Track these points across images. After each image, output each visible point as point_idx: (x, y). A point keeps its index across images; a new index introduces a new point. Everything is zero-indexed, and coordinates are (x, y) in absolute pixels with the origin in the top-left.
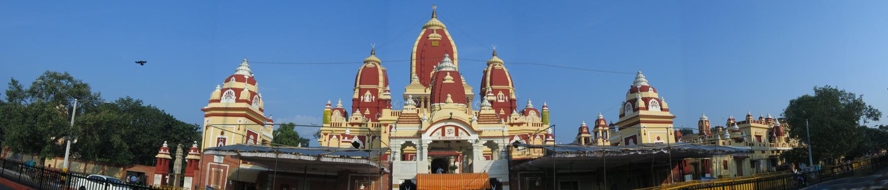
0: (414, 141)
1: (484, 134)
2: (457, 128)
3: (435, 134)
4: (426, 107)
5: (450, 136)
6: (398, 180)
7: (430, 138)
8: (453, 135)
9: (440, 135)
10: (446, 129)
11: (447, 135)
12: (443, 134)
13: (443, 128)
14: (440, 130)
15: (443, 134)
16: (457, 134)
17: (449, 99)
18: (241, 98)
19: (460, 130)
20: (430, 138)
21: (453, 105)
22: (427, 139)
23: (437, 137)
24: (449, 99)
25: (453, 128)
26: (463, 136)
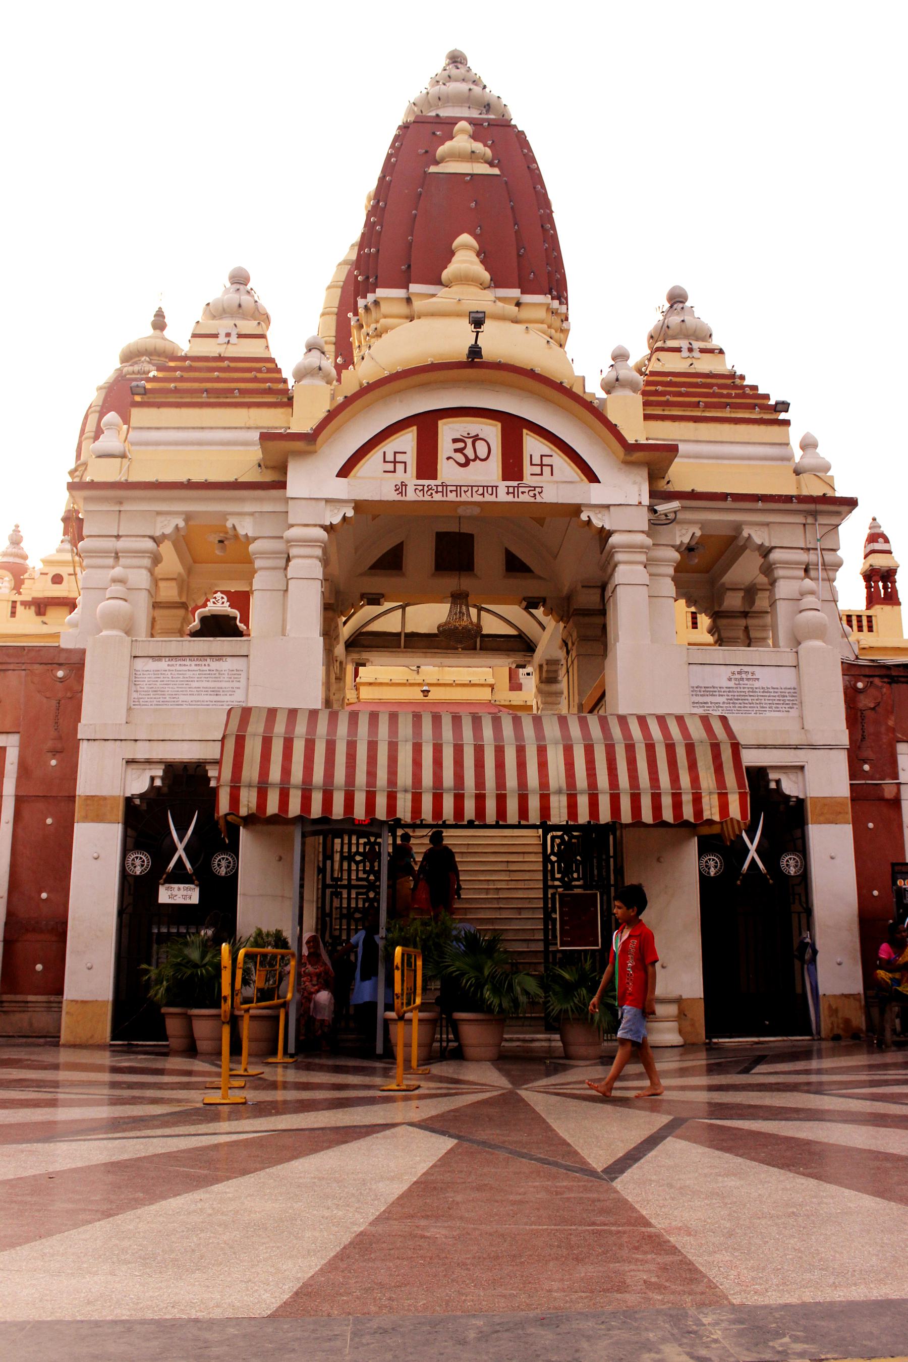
0: (246, 519)
1: (683, 475)
2: (513, 428)
3: (373, 463)
5: (472, 476)
6: (107, 773)
7: (342, 489)
8: (495, 465)
11: (448, 471)
12: (427, 466)
13: (426, 425)
14: (407, 442)
16: (512, 467)
19: (533, 446)
20: (342, 489)
25: (492, 432)
26: (556, 484)
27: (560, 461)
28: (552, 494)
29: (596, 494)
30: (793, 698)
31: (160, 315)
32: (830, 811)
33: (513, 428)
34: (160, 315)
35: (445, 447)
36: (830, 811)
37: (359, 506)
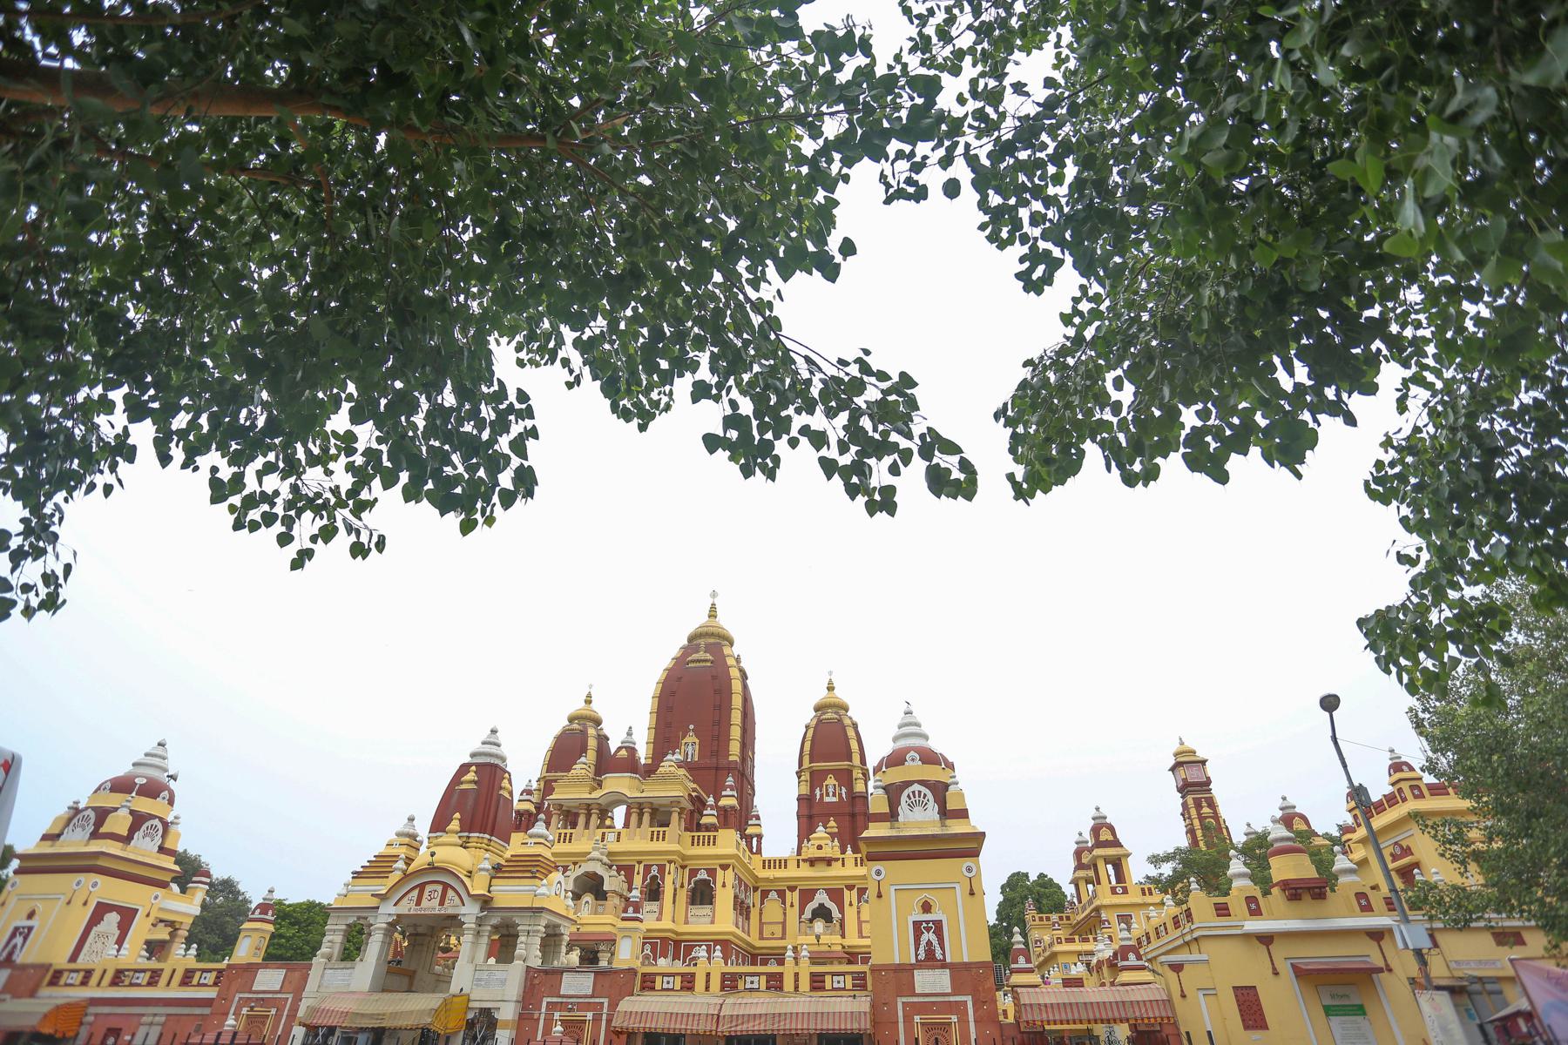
4: (587, 826)
5: (431, 906)
9: (413, 904)
10: (428, 888)
11: (425, 903)
12: (418, 903)
13: (422, 887)
14: (415, 893)
15: (418, 903)
16: (442, 903)
17: (455, 825)
18: (102, 830)
19: (450, 893)
20: (393, 910)
21: (454, 839)
22: (389, 910)
23: (408, 907)
24: (455, 825)
25: (439, 888)
27: (457, 898)
28: (450, 911)
29: (463, 910)
30: (503, 982)
31: (589, 696)
32: (506, 1025)
33: (446, 886)
34: (589, 696)
35: (426, 894)
36: (506, 1025)
37: (399, 916)
